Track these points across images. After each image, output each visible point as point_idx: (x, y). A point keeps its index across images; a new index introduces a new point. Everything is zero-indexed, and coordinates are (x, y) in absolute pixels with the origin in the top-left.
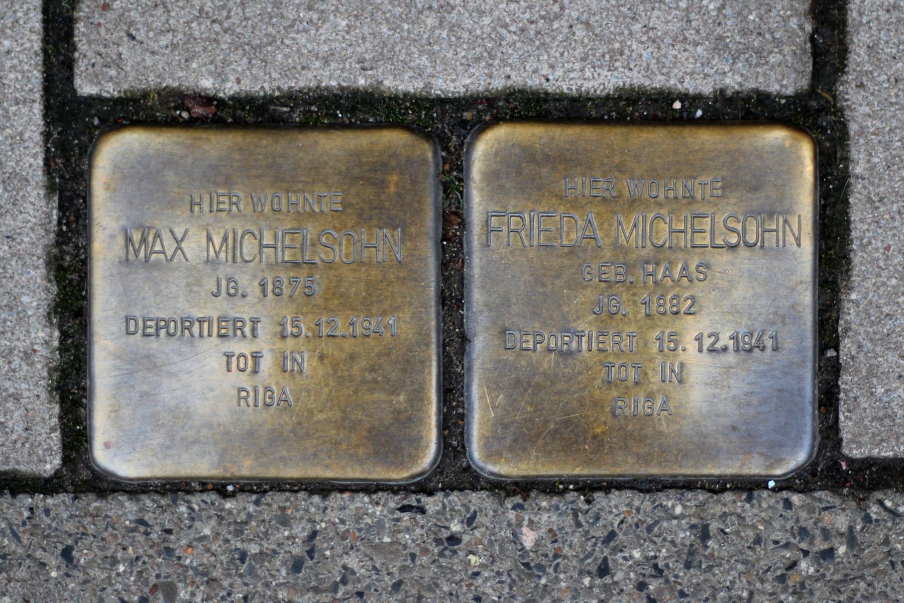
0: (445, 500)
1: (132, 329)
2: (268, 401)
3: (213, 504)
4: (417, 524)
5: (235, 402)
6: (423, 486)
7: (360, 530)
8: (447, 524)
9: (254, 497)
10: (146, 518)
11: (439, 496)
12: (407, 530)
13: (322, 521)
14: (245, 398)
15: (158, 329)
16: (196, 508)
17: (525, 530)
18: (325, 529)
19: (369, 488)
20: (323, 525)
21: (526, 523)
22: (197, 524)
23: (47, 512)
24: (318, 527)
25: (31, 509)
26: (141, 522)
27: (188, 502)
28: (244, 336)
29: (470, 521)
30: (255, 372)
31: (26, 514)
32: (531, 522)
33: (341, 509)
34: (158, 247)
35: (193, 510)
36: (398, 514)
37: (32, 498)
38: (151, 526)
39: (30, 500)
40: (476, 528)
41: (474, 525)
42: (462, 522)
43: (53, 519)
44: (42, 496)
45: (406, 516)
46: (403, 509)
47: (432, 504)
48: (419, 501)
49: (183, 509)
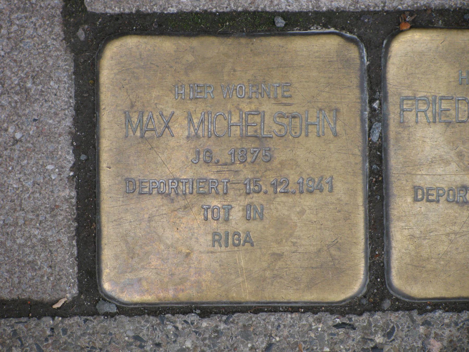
0: (371, 319)
1: (420, 197)
2: (237, 242)
3: (192, 323)
4: (349, 337)
5: (210, 243)
6: (351, 307)
7: (305, 342)
8: (372, 337)
9: (224, 318)
10: (141, 335)
11: (365, 316)
12: (342, 342)
13: (276, 335)
14: (219, 241)
15: (439, 196)
16: (180, 327)
17: (432, 341)
18: (279, 341)
19: (313, 308)
20: (278, 339)
21: (433, 335)
22: (180, 339)
23: (65, 331)
24: (274, 340)
25: (52, 329)
26: (137, 338)
27: (174, 322)
28: (217, 193)
29: (389, 335)
30: (227, 220)
31: (48, 333)
32: (436, 334)
33: (291, 326)
34: (150, 127)
35: (177, 328)
36: (334, 330)
37: (53, 320)
38: (145, 342)
39: (51, 321)
40: (394, 340)
41: (393, 338)
42: (384, 336)
43: (69, 337)
44: (60, 318)
45: (341, 331)
46: (338, 326)
47: (361, 321)
48: (350, 319)
49: (170, 327)
